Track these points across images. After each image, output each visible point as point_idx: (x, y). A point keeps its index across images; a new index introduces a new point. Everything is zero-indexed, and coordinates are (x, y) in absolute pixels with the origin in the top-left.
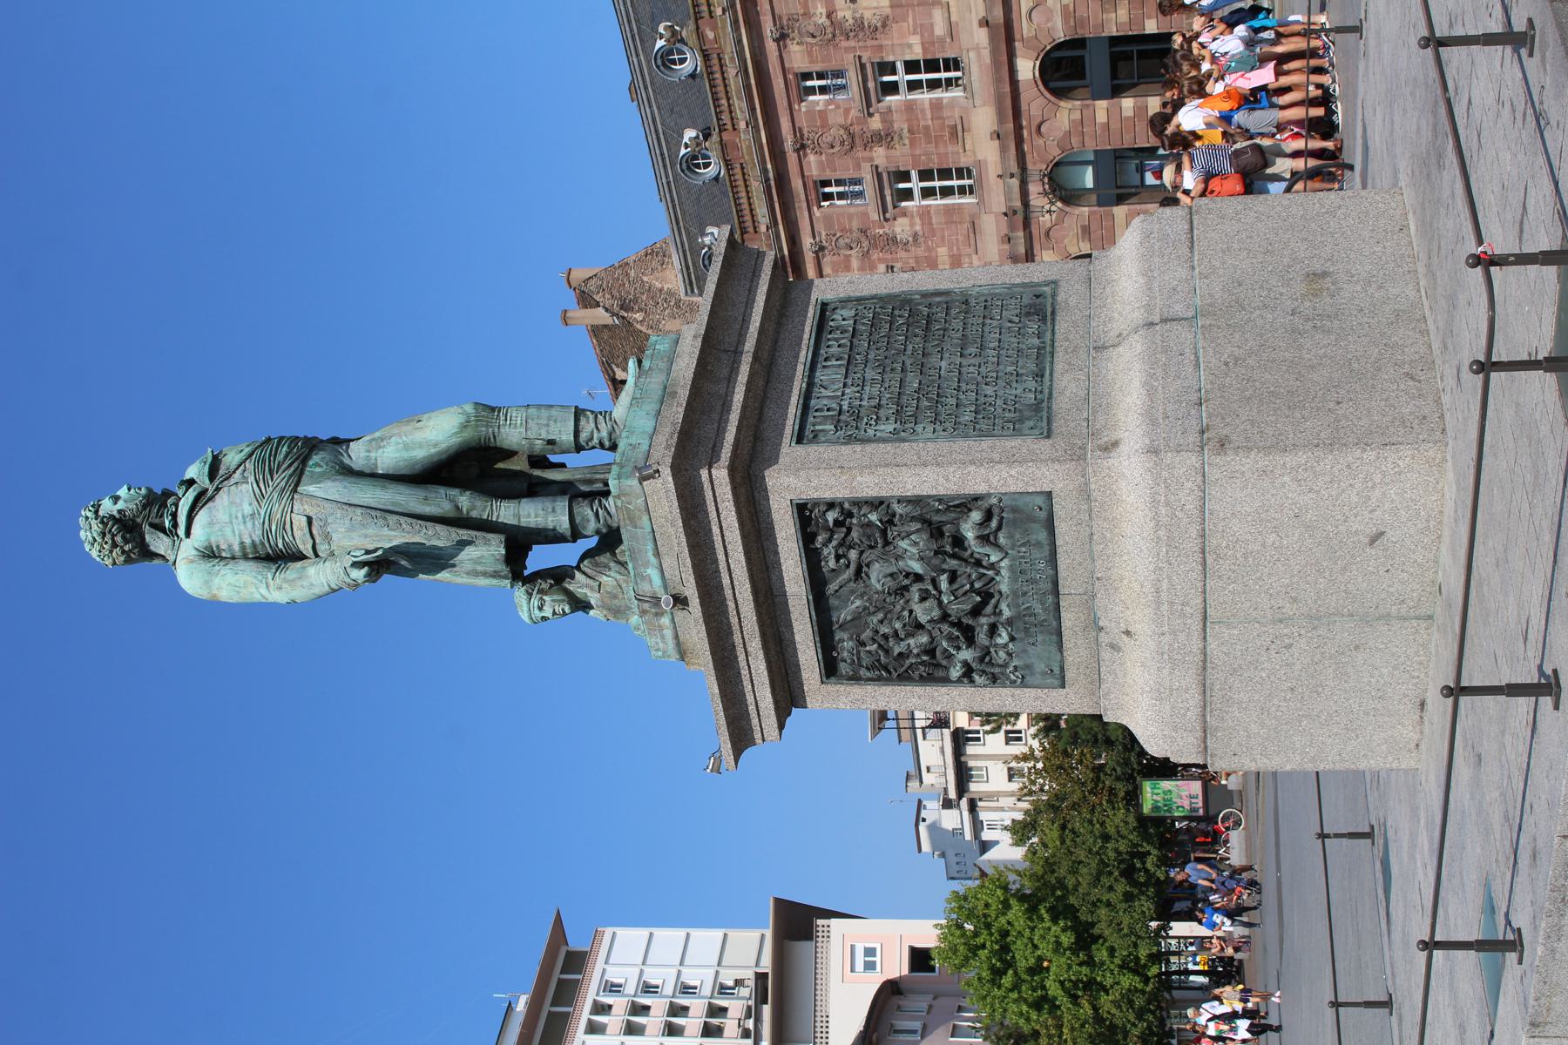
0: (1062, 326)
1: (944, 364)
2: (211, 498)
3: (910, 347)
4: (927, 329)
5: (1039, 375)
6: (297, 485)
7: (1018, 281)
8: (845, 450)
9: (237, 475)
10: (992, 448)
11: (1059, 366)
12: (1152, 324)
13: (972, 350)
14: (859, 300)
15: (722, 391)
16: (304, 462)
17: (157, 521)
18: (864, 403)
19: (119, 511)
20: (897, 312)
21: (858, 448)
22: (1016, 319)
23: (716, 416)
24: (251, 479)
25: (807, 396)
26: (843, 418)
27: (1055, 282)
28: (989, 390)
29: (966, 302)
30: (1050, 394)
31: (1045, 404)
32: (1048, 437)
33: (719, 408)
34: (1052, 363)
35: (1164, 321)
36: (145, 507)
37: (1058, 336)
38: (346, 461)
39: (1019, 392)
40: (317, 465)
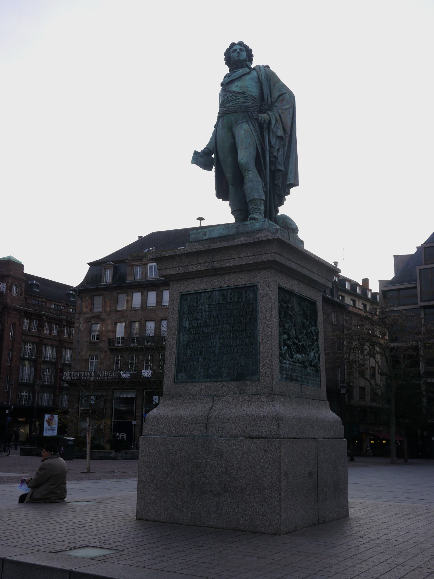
0: (232, 384)
3: (228, 326)
5: (208, 377)
11: (209, 384)
12: (208, 419)
14: (256, 300)
18: (200, 314)
20: (249, 317)
21: (176, 317)
27: (259, 380)
28: (200, 359)
29: (252, 344)
30: (196, 382)
31: (192, 380)
32: (174, 382)
34: (211, 381)
35: (206, 425)
37: (225, 383)
39: (199, 370)
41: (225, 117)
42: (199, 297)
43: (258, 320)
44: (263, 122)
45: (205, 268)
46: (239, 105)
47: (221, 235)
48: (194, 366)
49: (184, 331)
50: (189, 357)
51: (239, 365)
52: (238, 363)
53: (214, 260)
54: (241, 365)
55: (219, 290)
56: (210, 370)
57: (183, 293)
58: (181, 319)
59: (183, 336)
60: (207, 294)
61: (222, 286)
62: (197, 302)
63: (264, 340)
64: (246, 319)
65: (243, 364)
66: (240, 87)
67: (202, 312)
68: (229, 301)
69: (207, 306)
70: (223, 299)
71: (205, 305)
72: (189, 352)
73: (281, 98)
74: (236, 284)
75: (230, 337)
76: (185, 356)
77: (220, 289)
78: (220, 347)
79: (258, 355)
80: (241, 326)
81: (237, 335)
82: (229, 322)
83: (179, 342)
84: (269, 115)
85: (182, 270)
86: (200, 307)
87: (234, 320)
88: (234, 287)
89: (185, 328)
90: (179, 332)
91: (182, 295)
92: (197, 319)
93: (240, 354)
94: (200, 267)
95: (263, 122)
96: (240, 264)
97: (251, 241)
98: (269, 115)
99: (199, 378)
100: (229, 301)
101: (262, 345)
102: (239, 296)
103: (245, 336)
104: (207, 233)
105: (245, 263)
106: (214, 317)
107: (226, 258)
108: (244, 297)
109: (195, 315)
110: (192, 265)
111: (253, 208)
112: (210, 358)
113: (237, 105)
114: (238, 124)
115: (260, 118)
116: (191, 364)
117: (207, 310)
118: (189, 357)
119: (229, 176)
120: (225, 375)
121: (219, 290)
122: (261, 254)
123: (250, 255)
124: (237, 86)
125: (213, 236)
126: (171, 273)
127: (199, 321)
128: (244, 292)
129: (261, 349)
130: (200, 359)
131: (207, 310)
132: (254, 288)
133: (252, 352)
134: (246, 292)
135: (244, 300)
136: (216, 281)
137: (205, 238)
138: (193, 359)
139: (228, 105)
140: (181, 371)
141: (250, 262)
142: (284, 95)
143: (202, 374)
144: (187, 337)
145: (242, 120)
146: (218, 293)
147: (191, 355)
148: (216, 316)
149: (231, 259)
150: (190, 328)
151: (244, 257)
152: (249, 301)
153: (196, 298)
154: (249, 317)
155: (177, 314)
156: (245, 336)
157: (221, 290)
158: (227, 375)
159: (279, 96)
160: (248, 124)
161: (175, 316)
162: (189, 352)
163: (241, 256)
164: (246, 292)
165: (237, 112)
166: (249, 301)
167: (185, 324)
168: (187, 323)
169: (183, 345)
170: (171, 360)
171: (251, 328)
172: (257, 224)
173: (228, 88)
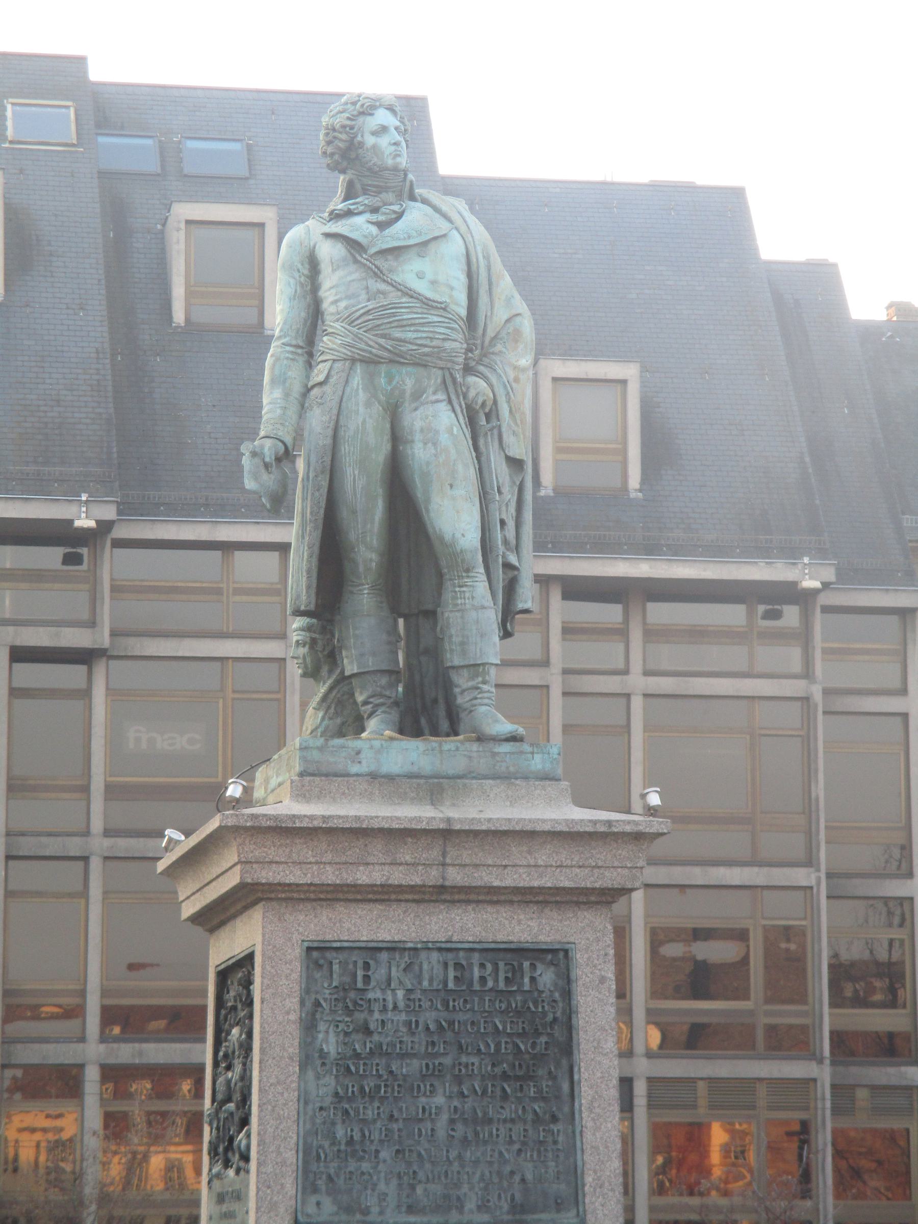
1: (439, 1100)
2: (356, 261)
3: (475, 1060)
4: (505, 1076)
6: (361, 361)
7: (589, 1179)
8: (293, 1003)
9: (383, 287)
10: (284, 1163)
13: (460, 1129)
14: (567, 994)
15: (371, 859)
16: (391, 361)
17: (358, 186)
18: (377, 1015)
19: (361, 144)
20: (543, 1039)
21: (293, 1017)
22: (517, 1178)
23: (328, 857)
24: (371, 305)
25: (393, 948)
26: (352, 995)
29: (554, 1119)
33: (343, 859)
36: (370, 169)
38: (407, 406)
39: (382, 1186)
40: (390, 379)
41: (383, 368)
42: (371, 962)
43: (575, 1052)
44: (478, 407)
45: (416, 880)
46: (435, 343)
47: (415, 769)
48: (363, 1173)
49: (323, 1064)
50: (343, 1147)
51: (517, 1178)
52: (512, 1173)
53: (448, 861)
54: (523, 1180)
55: (440, 950)
56: (419, 1190)
57: (315, 945)
58: (309, 1026)
59: (318, 1077)
60: (397, 956)
61: (455, 938)
62: (367, 979)
63: (597, 1110)
64: (534, 1045)
65: (529, 1176)
66: (434, 283)
67: (384, 1009)
68: (477, 987)
69: (400, 994)
70: (456, 977)
71: (393, 990)
72: (340, 1132)
73: (510, 328)
74: (500, 937)
75: (484, 1092)
76: (326, 1144)
77: (449, 945)
78: (452, 1121)
79: (579, 1153)
80: (520, 1065)
81: (509, 1090)
82: (479, 1050)
83: (304, 1099)
84: (491, 386)
85: (330, 876)
86: (378, 994)
87: (498, 1045)
88: (493, 946)
89: (323, 1055)
90: (303, 1067)
91: (309, 949)
92: (367, 1031)
93: (516, 1147)
94: (398, 877)
95: (478, 407)
96: (536, 884)
97: (587, 829)
98: (491, 386)
99: (381, 1213)
100: (477, 987)
101: (590, 1124)
102: (510, 975)
103: (532, 1094)
104: (362, 756)
105: (549, 885)
106: (428, 1029)
107: (490, 862)
108: (527, 980)
109: (360, 1016)
110: (368, 864)
111: (477, 688)
112: (419, 1155)
113: (428, 342)
114: (423, 404)
115: (472, 394)
116: (351, 1168)
117: (401, 1005)
118: (343, 1147)
120: (470, 1205)
121: (440, 950)
122: (599, 867)
123: (569, 862)
124: (420, 276)
125: (385, 769)
126: (290, 879)
127: (376, 1037)
128: (526, 964)
129: (588, 1136)
130: (384, 1154)
131: (401, 1005)
132: (558, 957)
133: (555, 1142)
134: (533, 966)
135: (527, 987)
136: (434, 919)
137: (354, 769)
138: (361, 1153)
139: (397, 334)
140: (315, 1190)
141: (567, 884)
142: (518, 319)
143: (392, 1200)
144: (333, 1083)
145: (434, 393)
146: (435, 955)
147: (350, 1142)
148: (432, 1027)
149: (506, 866)
150: (342, 1057)
151: (546, 866)
152: (543, 992)
153: (360, 964)
154: (543, 1039)
155: (297, 1007)
156: (532, 1094)
158: (479, 1208)
159: (508, 321)
160: (454, 411)
161: (288, 1013)
162: (340, 1132)
163: (540, 862)
164: (533, 966)
165: (425, 366)
166: (543, 992)
167: (326, 1040)
168: (332, 1038)
169: (321, 1109)
170: (279, 1153)
171: (550, 1073)
172: (538, 757)
173: (390, 271)
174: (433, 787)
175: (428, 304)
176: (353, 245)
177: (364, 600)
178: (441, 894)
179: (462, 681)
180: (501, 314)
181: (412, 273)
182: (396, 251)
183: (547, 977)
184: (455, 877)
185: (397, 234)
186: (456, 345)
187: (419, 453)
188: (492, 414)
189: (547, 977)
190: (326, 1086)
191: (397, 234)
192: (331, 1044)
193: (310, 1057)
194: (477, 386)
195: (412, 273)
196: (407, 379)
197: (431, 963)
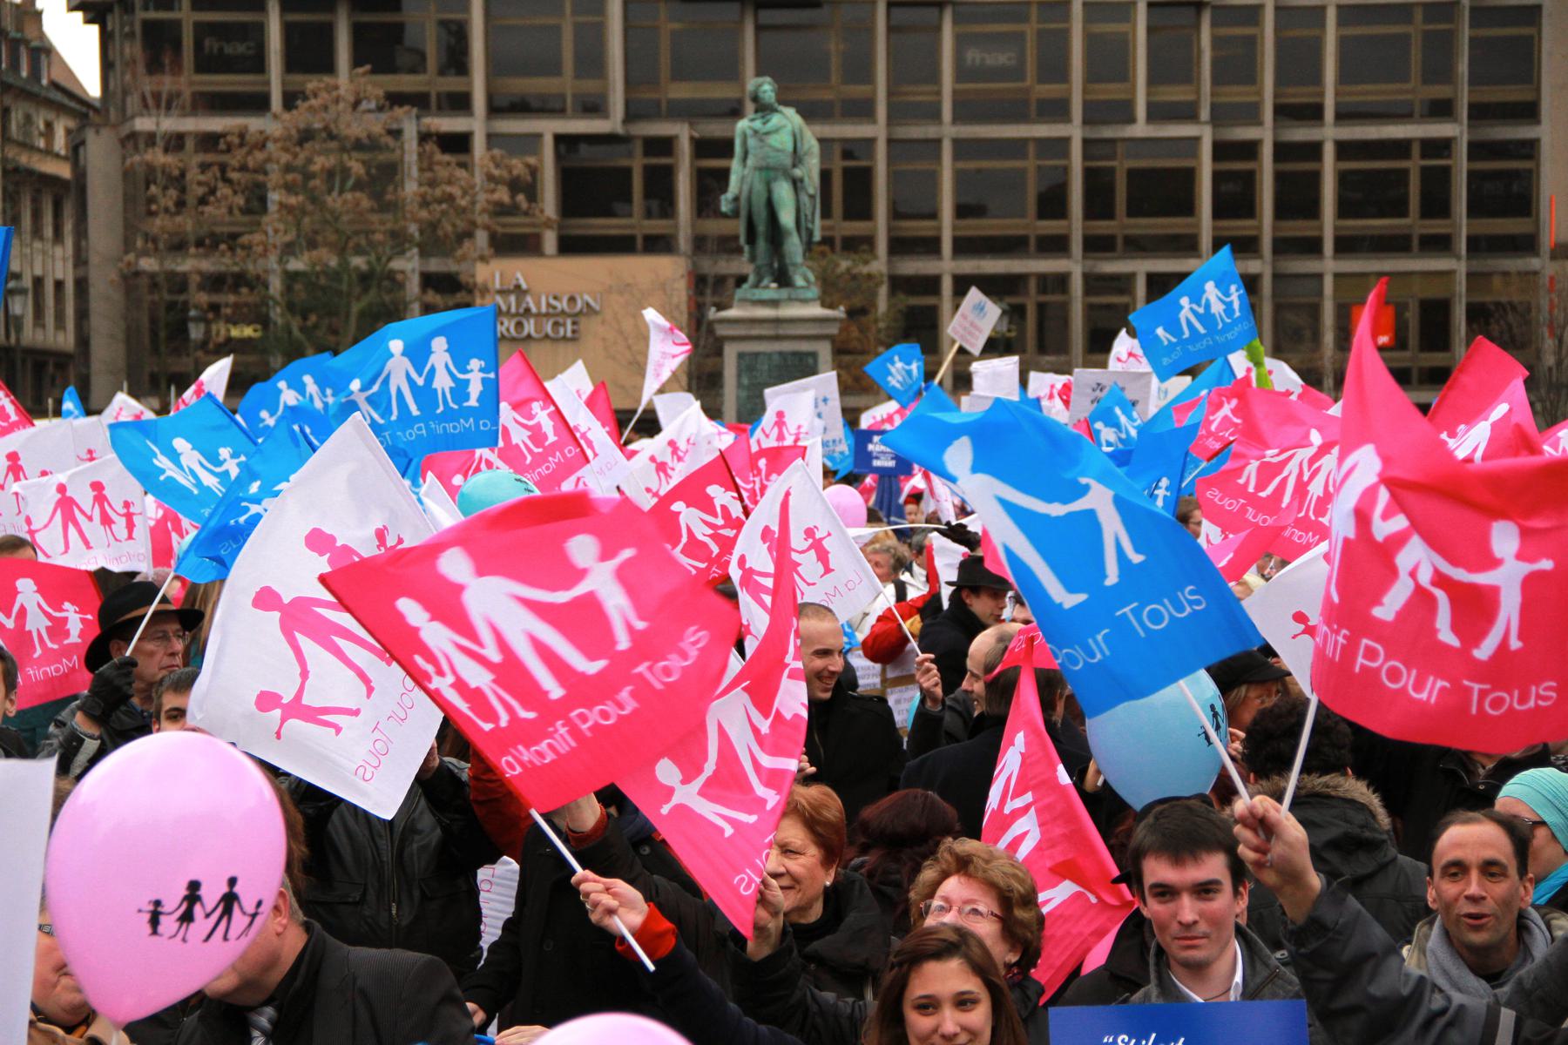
58: (739, 376)
83: (738, 398)
119: (761, 228)
157: (781, 353)
174: (774, 303)
175: (778, 150)
176: (756, 132)
177: (762, 245)
178: (777, 338)
179: (791, 269)
180: (806, 147)
181: (774, 140)
182: (768, 133)
183: (810, 361)
184: (781, 332)
185: (770, 126)
186: (788, 161)
187: (776, 196)
188: (802, 180)
189: (810, 361)
190: (744, 394)
191: (770, 126)
192: (745, 381)
193: (740, 385)
194: (798, 172)
195: (774, 140)
196: (772, 174)
197: (776, 357)
